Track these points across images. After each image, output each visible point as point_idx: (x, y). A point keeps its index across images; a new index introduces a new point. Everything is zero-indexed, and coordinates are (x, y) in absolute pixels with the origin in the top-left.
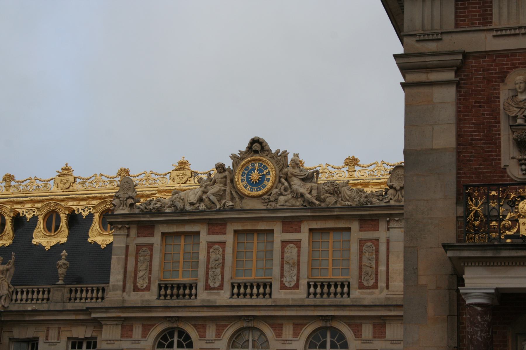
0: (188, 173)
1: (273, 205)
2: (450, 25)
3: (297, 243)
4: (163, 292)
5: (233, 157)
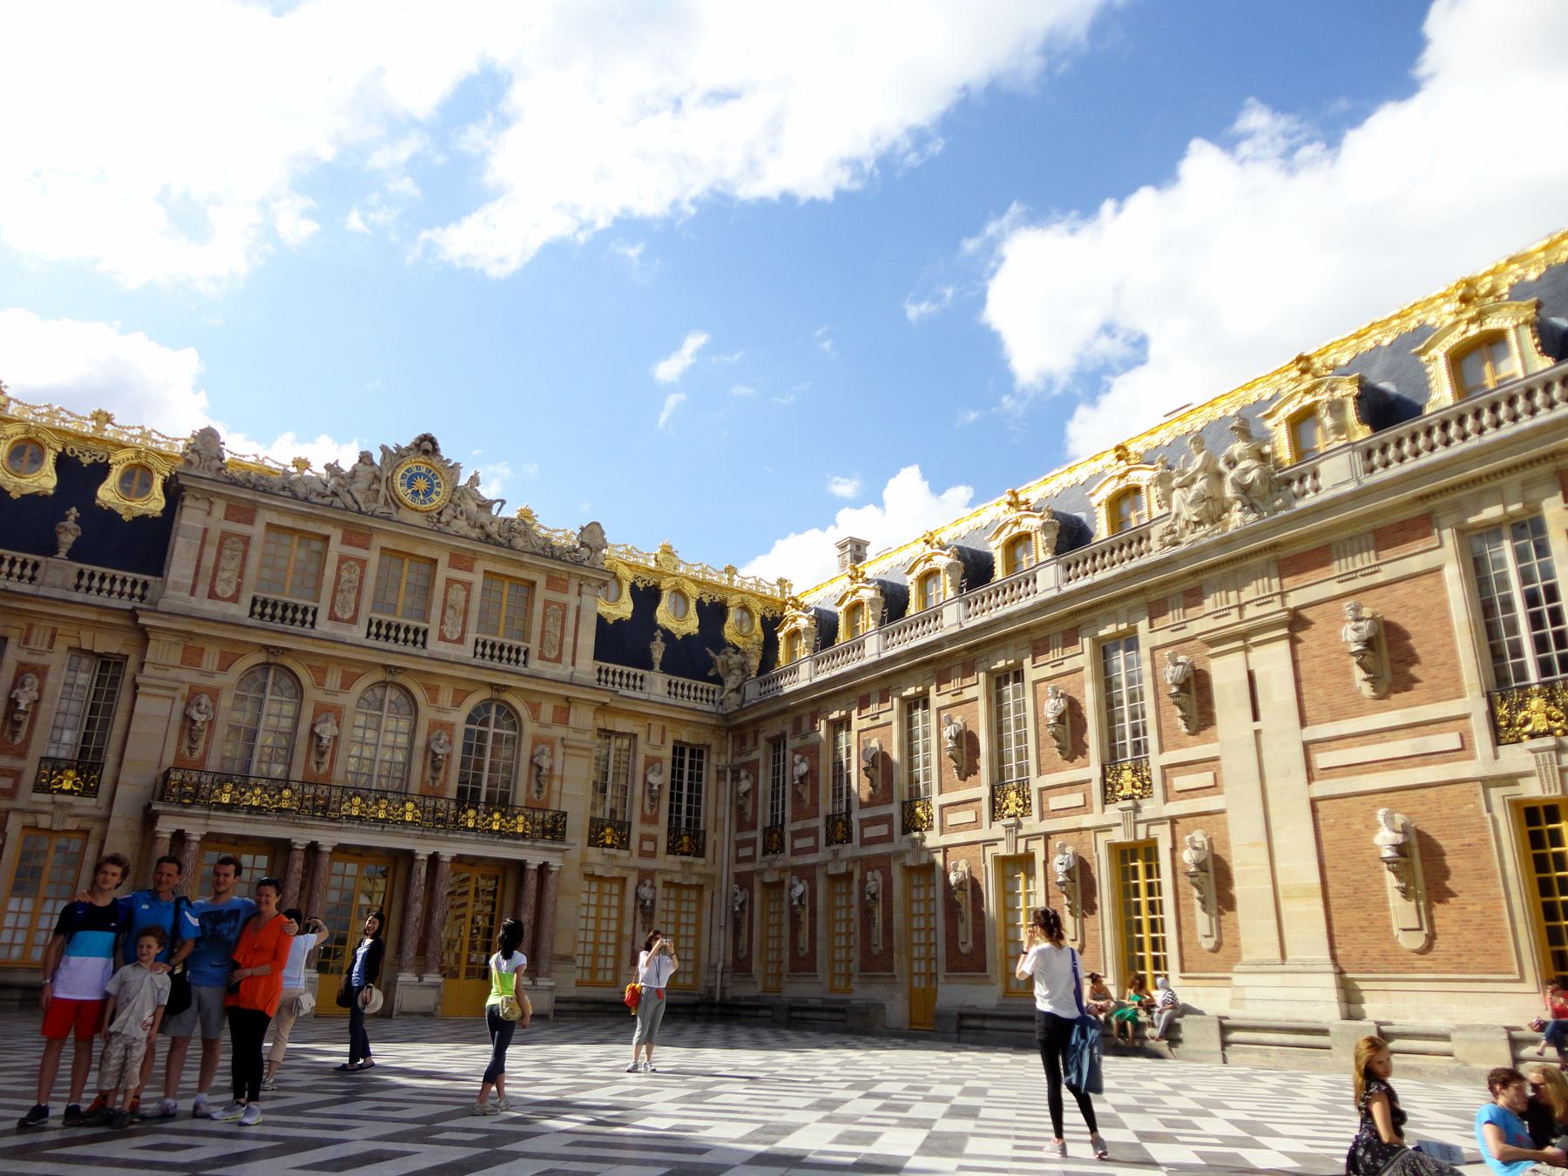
3: (468, 586)
4: (258, 609)
5: (384, 448)
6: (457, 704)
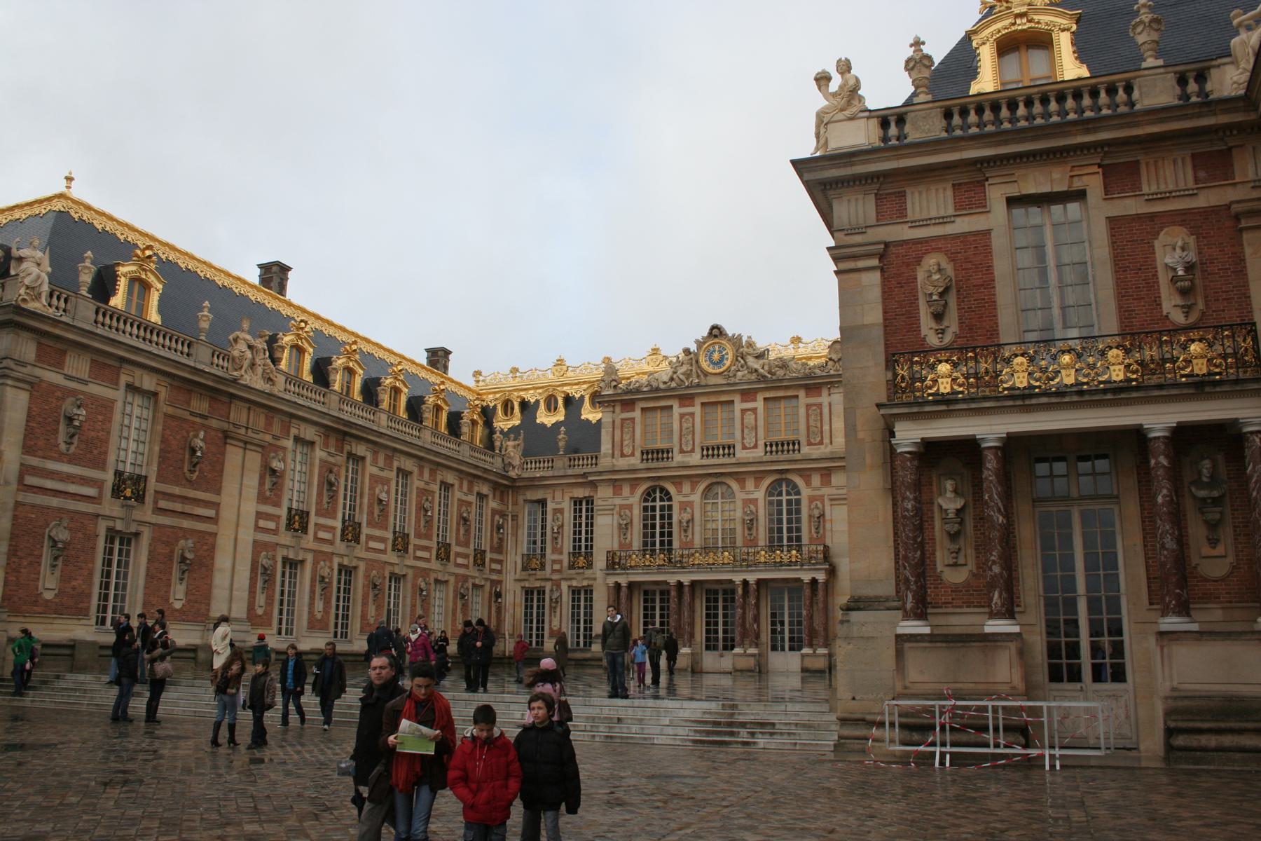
0: (660, 358)
1: (732, 380)
2: (872, 220)
3: (754, 410)
5: (697, 342)
6: (757, 486)
